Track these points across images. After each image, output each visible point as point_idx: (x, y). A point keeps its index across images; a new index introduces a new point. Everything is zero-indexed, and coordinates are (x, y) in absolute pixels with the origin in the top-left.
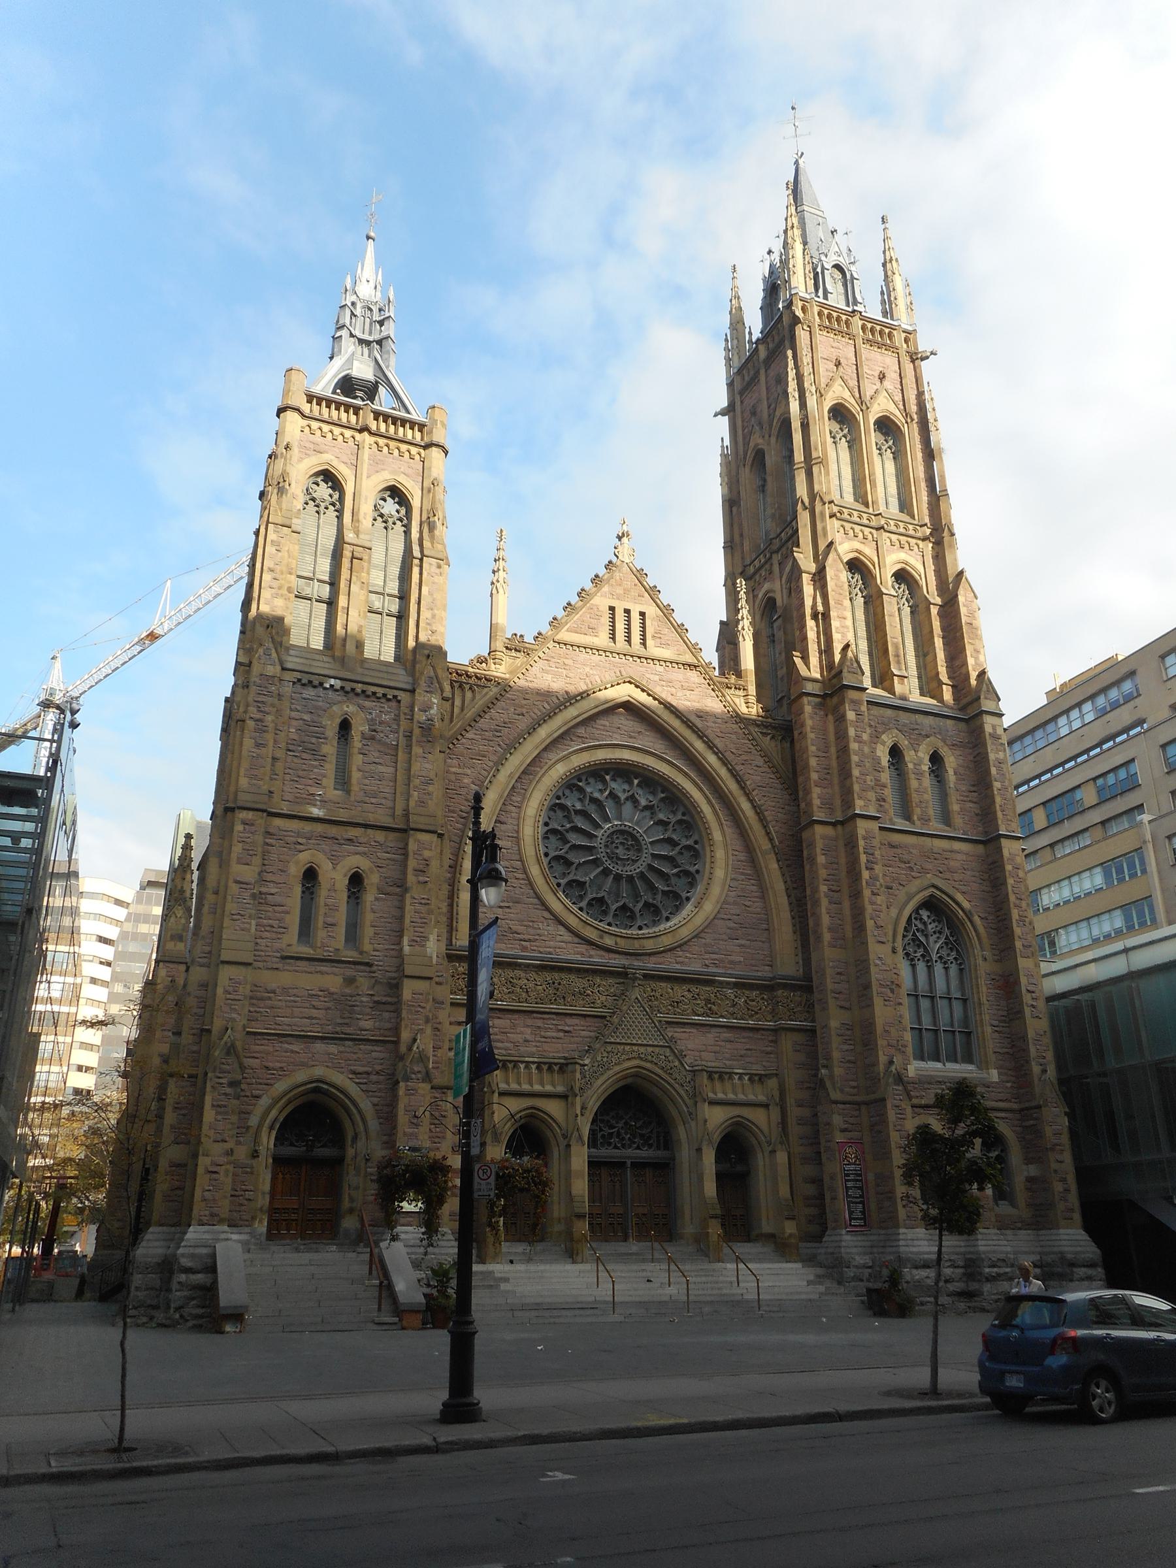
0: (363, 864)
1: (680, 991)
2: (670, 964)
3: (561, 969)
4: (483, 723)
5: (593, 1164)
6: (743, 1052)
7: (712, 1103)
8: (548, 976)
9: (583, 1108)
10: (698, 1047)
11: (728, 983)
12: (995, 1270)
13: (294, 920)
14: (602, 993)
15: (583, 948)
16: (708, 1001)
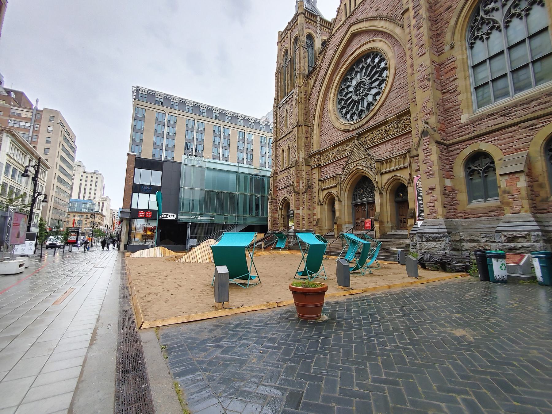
0: (289, 143)
1: (376, 132)
2: (373, 123)
3: (338, 145)
4: (317, 83)
5: (355, 206)
6: (402, 147)
7: (381, 174)
8: (335, 149)
9: (341, 189)
10: (381, 152)
11: (394, 119)
12: (513, 244)
13: (281, 163)
14: (348, 147)
15: (345, 135)
16: (386, 131)
